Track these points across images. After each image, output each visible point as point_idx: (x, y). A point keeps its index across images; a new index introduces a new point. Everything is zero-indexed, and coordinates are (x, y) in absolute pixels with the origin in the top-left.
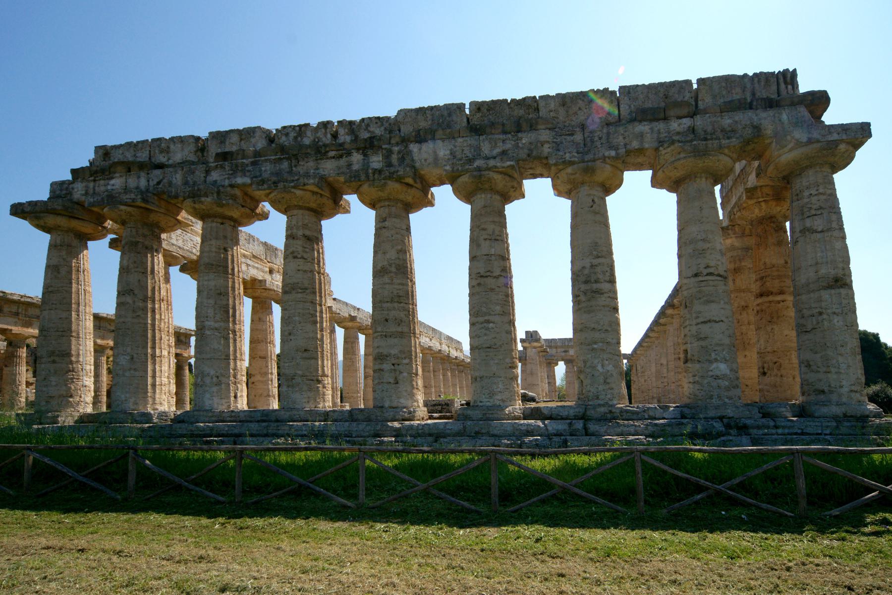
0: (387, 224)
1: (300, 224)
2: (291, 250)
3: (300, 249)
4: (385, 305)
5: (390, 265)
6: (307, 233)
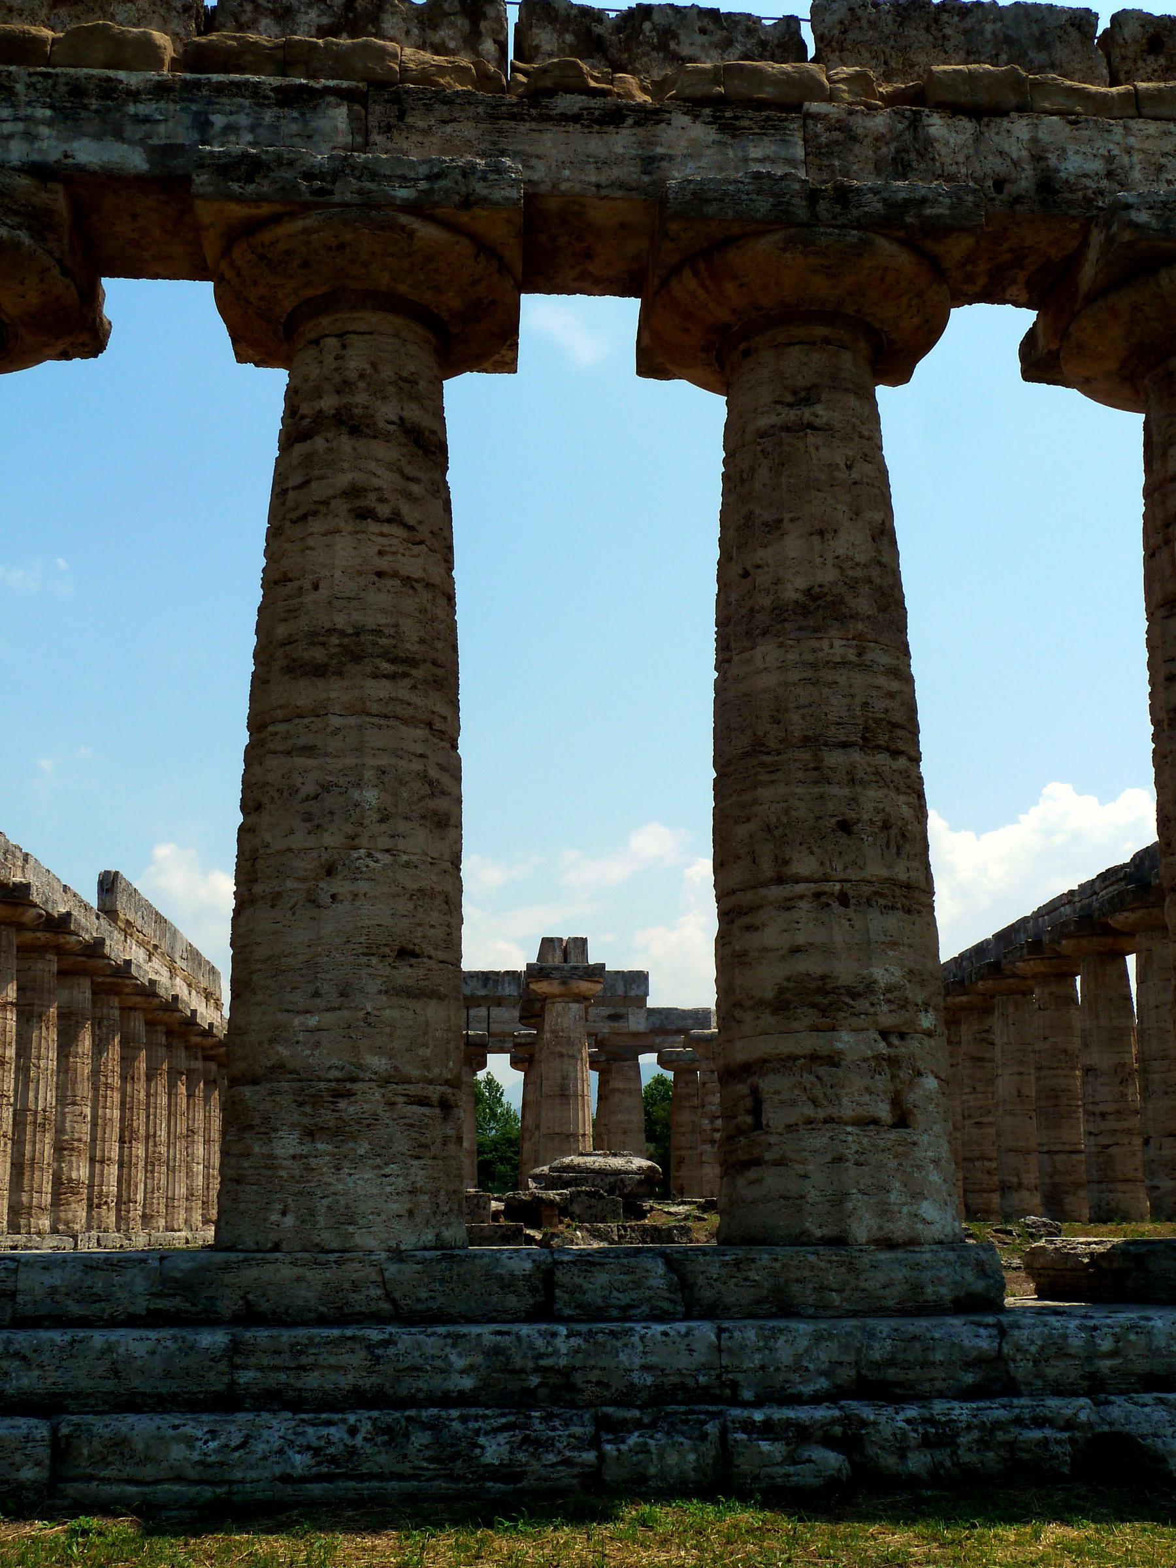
0: (822, 413)
1: (387, 372)
2: (344, 480)
3: (386, 479)
4: (834, 758)
5: (853, 585)
6: (413, 413)
